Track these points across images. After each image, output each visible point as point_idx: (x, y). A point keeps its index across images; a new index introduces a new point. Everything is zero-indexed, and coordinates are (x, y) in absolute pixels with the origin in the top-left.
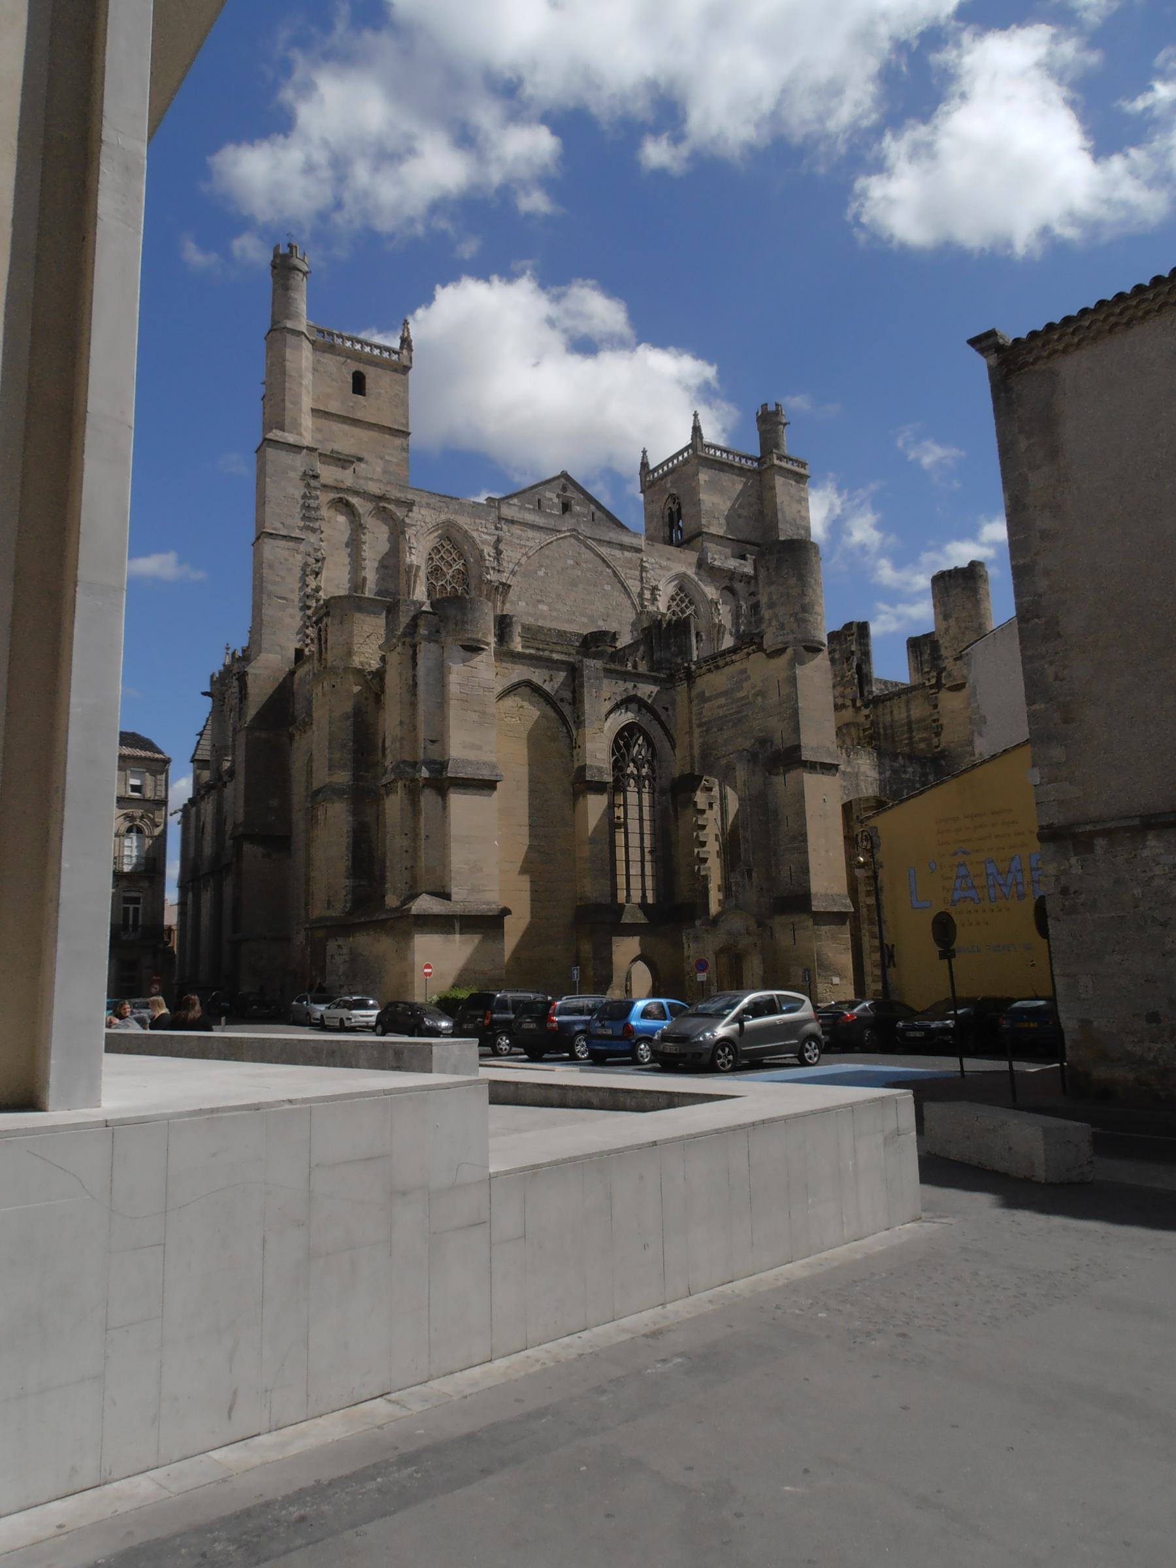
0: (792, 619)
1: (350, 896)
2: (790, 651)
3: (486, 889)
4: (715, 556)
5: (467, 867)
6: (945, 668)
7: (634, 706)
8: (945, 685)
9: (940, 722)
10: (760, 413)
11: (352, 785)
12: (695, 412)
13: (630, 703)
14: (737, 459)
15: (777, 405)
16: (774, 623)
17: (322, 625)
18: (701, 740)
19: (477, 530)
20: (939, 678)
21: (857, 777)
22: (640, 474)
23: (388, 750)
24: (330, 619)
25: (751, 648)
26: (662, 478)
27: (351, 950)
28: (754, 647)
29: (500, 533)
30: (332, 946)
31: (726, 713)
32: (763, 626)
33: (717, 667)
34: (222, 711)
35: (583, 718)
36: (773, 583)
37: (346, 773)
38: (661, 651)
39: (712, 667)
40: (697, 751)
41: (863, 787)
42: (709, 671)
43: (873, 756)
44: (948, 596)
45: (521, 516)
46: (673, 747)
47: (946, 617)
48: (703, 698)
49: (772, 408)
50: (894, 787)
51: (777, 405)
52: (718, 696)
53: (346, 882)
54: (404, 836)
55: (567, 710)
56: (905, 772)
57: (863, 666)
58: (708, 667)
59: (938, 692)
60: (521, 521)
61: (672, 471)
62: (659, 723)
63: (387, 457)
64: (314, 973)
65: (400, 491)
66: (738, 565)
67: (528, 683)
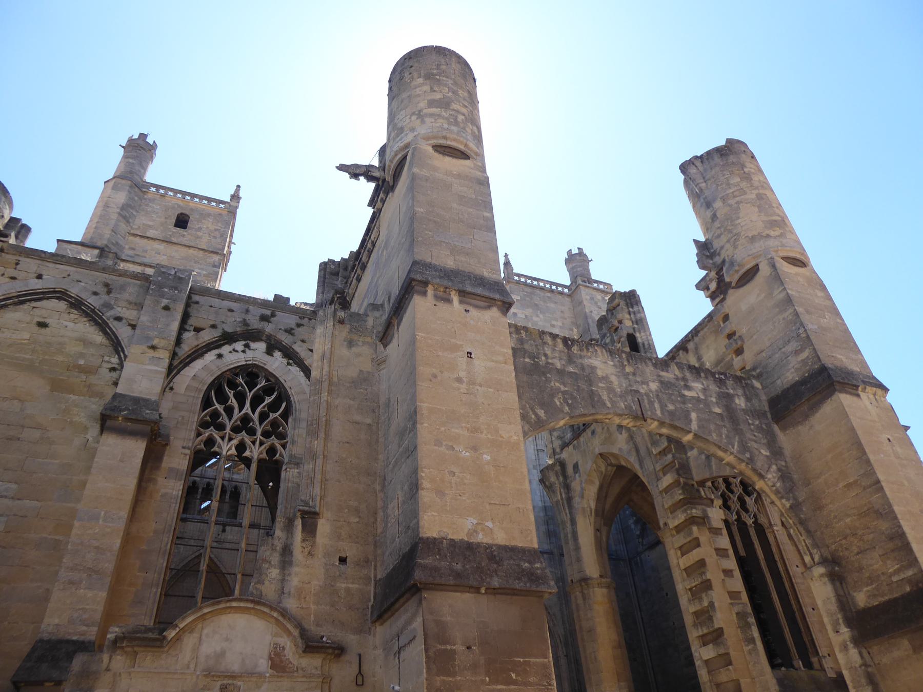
6: (724, 261)
7: (261, 346)
8: (731, 283)
9: (737, 335)
12: (506, 254)
14: (548, 286)
15: (579, 248)
21: (590, 382)
28: (382, 195)
33: (364, 267)
39: (359, 271)
41: (605, 397)
43: (620, 357)
47: (708, 205)
49: (575, 251)
50: (671, 407)
51: (579, 248)
56: (688, 387)
57: (637, 335)
67: (61, 295)
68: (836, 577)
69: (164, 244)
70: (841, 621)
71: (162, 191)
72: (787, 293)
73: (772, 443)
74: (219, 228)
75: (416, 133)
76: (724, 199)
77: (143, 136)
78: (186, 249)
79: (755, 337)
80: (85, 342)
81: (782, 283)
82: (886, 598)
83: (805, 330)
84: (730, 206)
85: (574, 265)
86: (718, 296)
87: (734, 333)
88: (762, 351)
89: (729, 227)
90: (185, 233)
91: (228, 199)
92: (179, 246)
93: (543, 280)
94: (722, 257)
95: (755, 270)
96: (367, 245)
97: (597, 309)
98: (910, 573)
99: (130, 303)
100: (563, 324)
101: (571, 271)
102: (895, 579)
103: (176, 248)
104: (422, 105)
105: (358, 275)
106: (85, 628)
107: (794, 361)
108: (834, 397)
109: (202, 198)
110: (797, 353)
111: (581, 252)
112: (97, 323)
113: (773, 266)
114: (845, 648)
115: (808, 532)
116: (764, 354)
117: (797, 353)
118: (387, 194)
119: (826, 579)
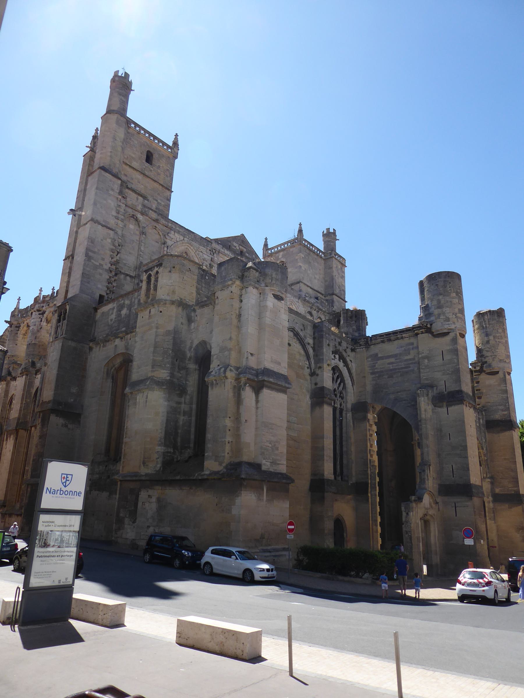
0: (454, 316)
1: (160, 460)
2: (452, 335)
3: (279, 462)
4: (307, 295)
5: (270, 445)
6: (486, 362)
9: (481, 391)
10: (325, 232)
11: (170, 380)
13: (336, 354)
15: (334, 229)
16: (442, 317)
17: (153, 273)
18: (375, 382)
19: (202, 252)
20: (482, 367)
22: (263, 249)
23: (215, 357)
24: (161, 269)
25: (421, 330)
26: (276, 253)
27: (159, 500)
28: (423, 330)
29: (213, 257)
30: (143, 495)
31: (397, 367)
32: (432, 318)
33: (390, 340)
34: (17, 333)
35: (321, 357)
36: (441, 294)
37: (165, 371)
38: (347, 327)
39: (385, 339)
40: (369, 388)
42: (383, 342)
44: (489, 324)
45: (223, 251)
46: (353, 385)
47: (487, 335)
48: (376, 357)
49: (331, 231)
51: (334, 229)
52: (389, 357)
53: (160, 449)
54: (229, 419)
55: (311, 351)
58: (382, 339)
59: (480, 375)
60: (223, 253)
61: (282, 250)
62: (347, 369)
63: (159, 201)
64: (121, 515)
65: (166, 221)
66: (315, 302)
68: (492, 483)
69: (142, 175)
70: (490, 495)
71: (138, 129)
72: (507, 389)
73: (485, 437)
74: (168, 169)
75: (456, 326)
76: (494, 337)
77: (127, 75)
78: (153, 182)
79: (488, 396)
80: (300, 354)
81: (506, 384)
82: (505, 493)
83: (509, 405)
84: (496, 342)
85: (329, 240)
86: (477, 372)
87: (480, 390)
88: (489, 403)
89: (493, 350)
90: (152, 169)
91: (171, 144)
92: (150, 179)
93: (315, 246)
94: (486, 360)
95: (497, 373)
96: (397, 335)
97: (338, 274)
98: (516, 489)
99: (310, 335)
100: (319, 277)
101: (325, 242)
102: (510, 489)
103: (148, 180)
104: (457, 310)
105: (384, 341)
106: (331, 476)
107: (500, 413)
108: (511, 431)
109: (160, 141)
110: (503, 410)
111: (334, 233)
112: (301, 345)
113: (505, 376)
114: (489, 502)
115: (488, 468)
116: (489, 404)
117: (503, 410)
118: (426, 332)
119: (489, 483)
